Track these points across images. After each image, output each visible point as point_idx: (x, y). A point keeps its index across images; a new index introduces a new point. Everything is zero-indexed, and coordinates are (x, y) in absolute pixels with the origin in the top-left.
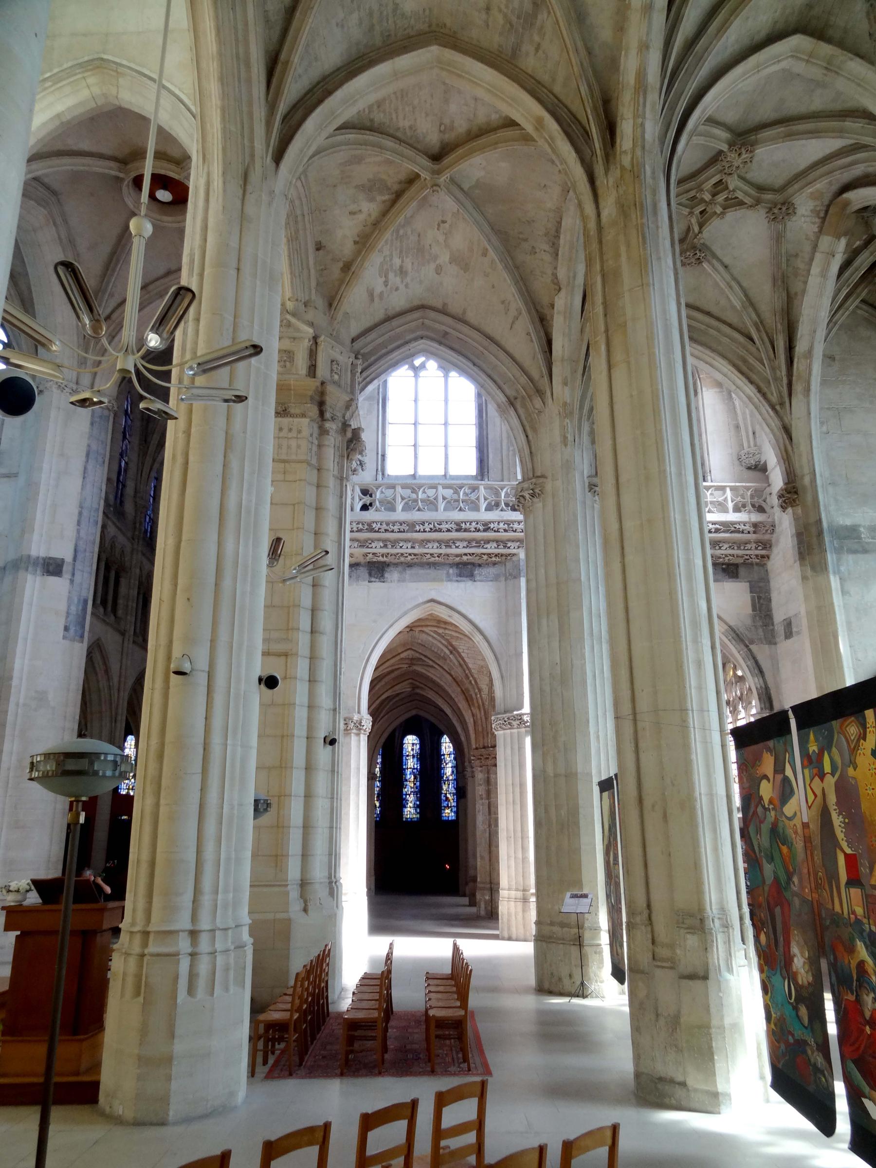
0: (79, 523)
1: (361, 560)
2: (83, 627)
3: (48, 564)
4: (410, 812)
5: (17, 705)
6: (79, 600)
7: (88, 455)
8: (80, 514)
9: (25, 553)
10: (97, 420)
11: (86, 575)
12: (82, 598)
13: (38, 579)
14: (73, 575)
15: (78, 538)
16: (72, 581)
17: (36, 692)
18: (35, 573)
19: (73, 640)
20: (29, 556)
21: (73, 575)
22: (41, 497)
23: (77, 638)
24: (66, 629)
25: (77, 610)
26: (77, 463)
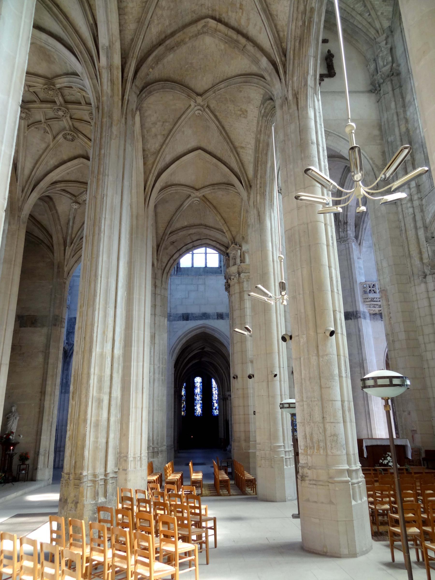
1: (377, 312)
4: (198, 409)
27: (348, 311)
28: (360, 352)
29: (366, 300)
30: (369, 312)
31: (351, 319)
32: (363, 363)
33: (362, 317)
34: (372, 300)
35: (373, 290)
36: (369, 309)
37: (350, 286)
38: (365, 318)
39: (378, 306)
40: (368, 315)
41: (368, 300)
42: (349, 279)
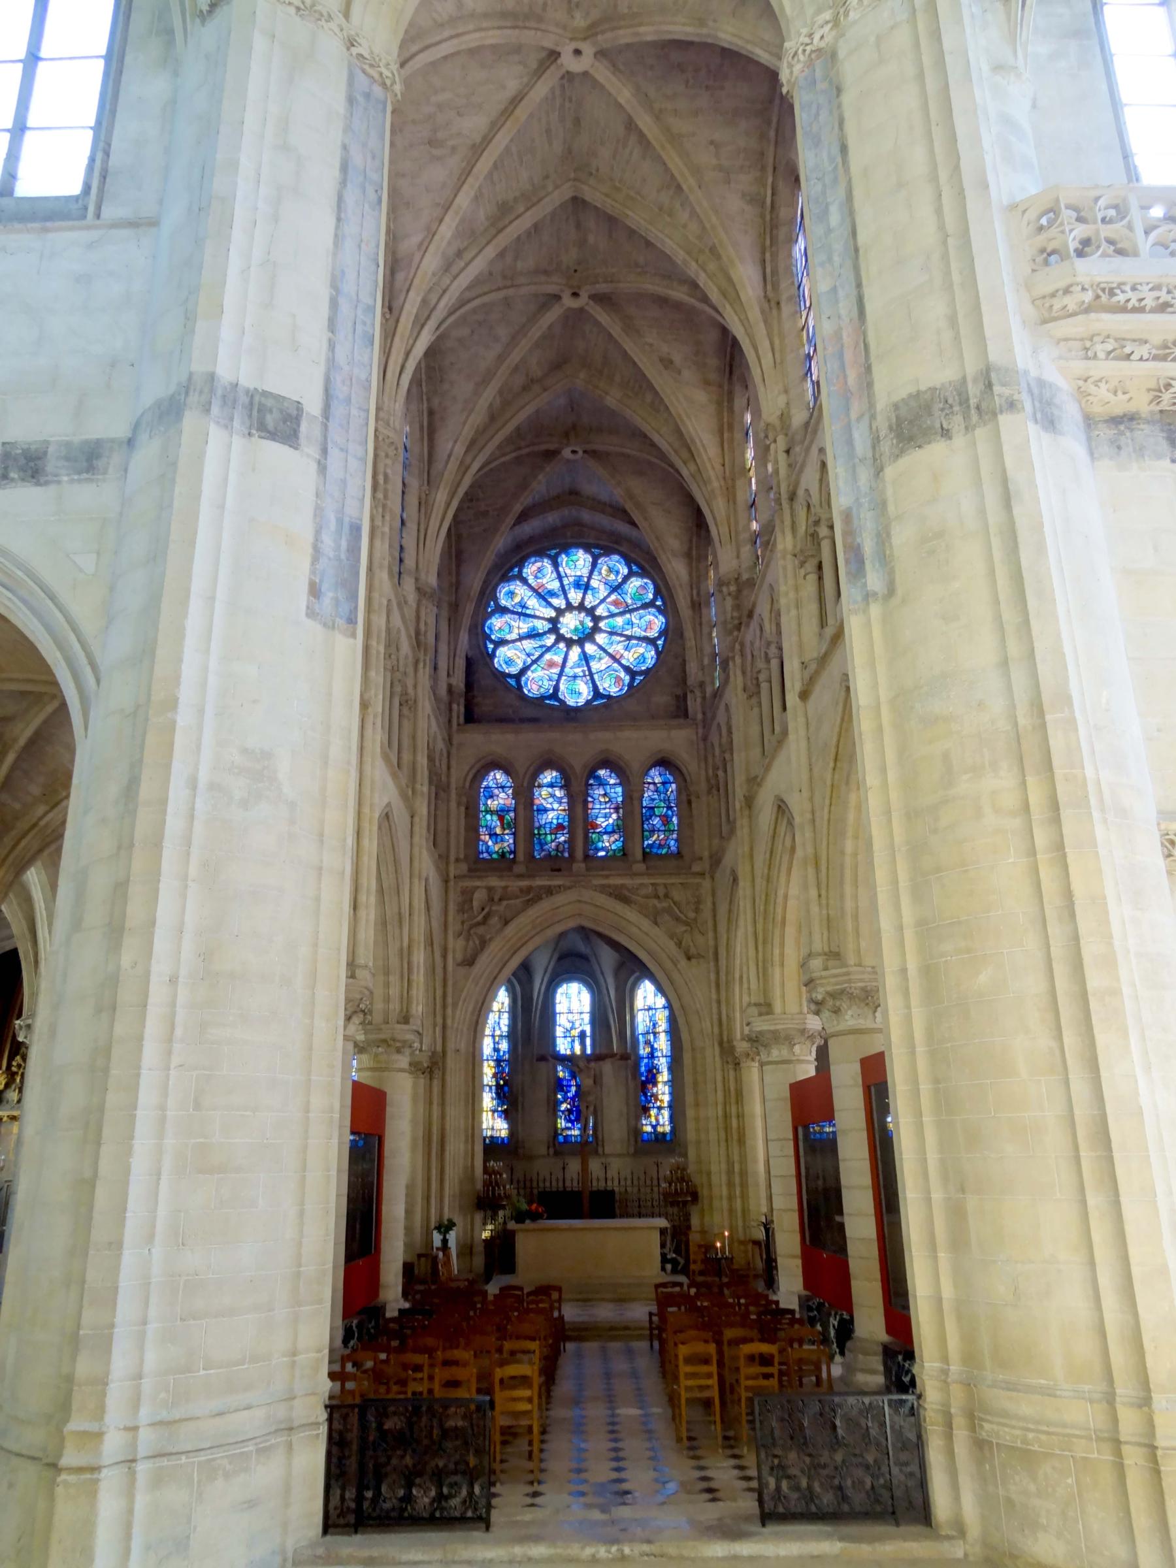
0: (332, 325)
2: (354, 597)
3: (262, 409)
5: (193, 784)
6: (340, 522)
7: (344, 168)
8: (334, 304)
9: (198, 367)
10: (360, 99)
11: (354, 464)
12: (347, 520)
13: (238, 442)
14: (324, 451)
15: (331, 364)
16: (322, 469)
17: (245, 751)
18: (228, 426)
19: (330, 626)
20: (212, 377)
21: (324, 451)
22: (238, 235)
23: (341, 622)
24: (315, 591)
25: (338, 548)
26: (323, 176)
27: (923, 388)
28: (1014, 649)
29: (1057, 304)
30: (1082, 395)
31: (946, 433)
32: (1043, 726)
33: (1028, 405)
34: (1105, 299)
35: (1111, 242)
36: (1079, 366)
37: (941, 227)
38: (1050, 423)
39: (1144, 351)
40: (1070, 413)
41: (1071, 302)
42: (934, 178)
